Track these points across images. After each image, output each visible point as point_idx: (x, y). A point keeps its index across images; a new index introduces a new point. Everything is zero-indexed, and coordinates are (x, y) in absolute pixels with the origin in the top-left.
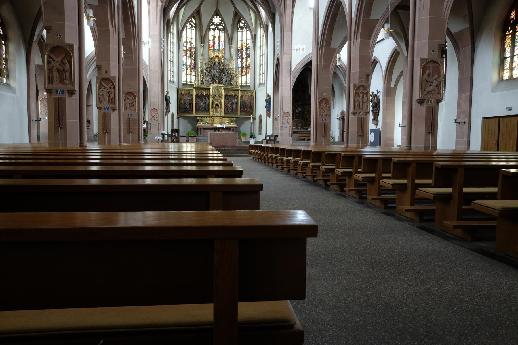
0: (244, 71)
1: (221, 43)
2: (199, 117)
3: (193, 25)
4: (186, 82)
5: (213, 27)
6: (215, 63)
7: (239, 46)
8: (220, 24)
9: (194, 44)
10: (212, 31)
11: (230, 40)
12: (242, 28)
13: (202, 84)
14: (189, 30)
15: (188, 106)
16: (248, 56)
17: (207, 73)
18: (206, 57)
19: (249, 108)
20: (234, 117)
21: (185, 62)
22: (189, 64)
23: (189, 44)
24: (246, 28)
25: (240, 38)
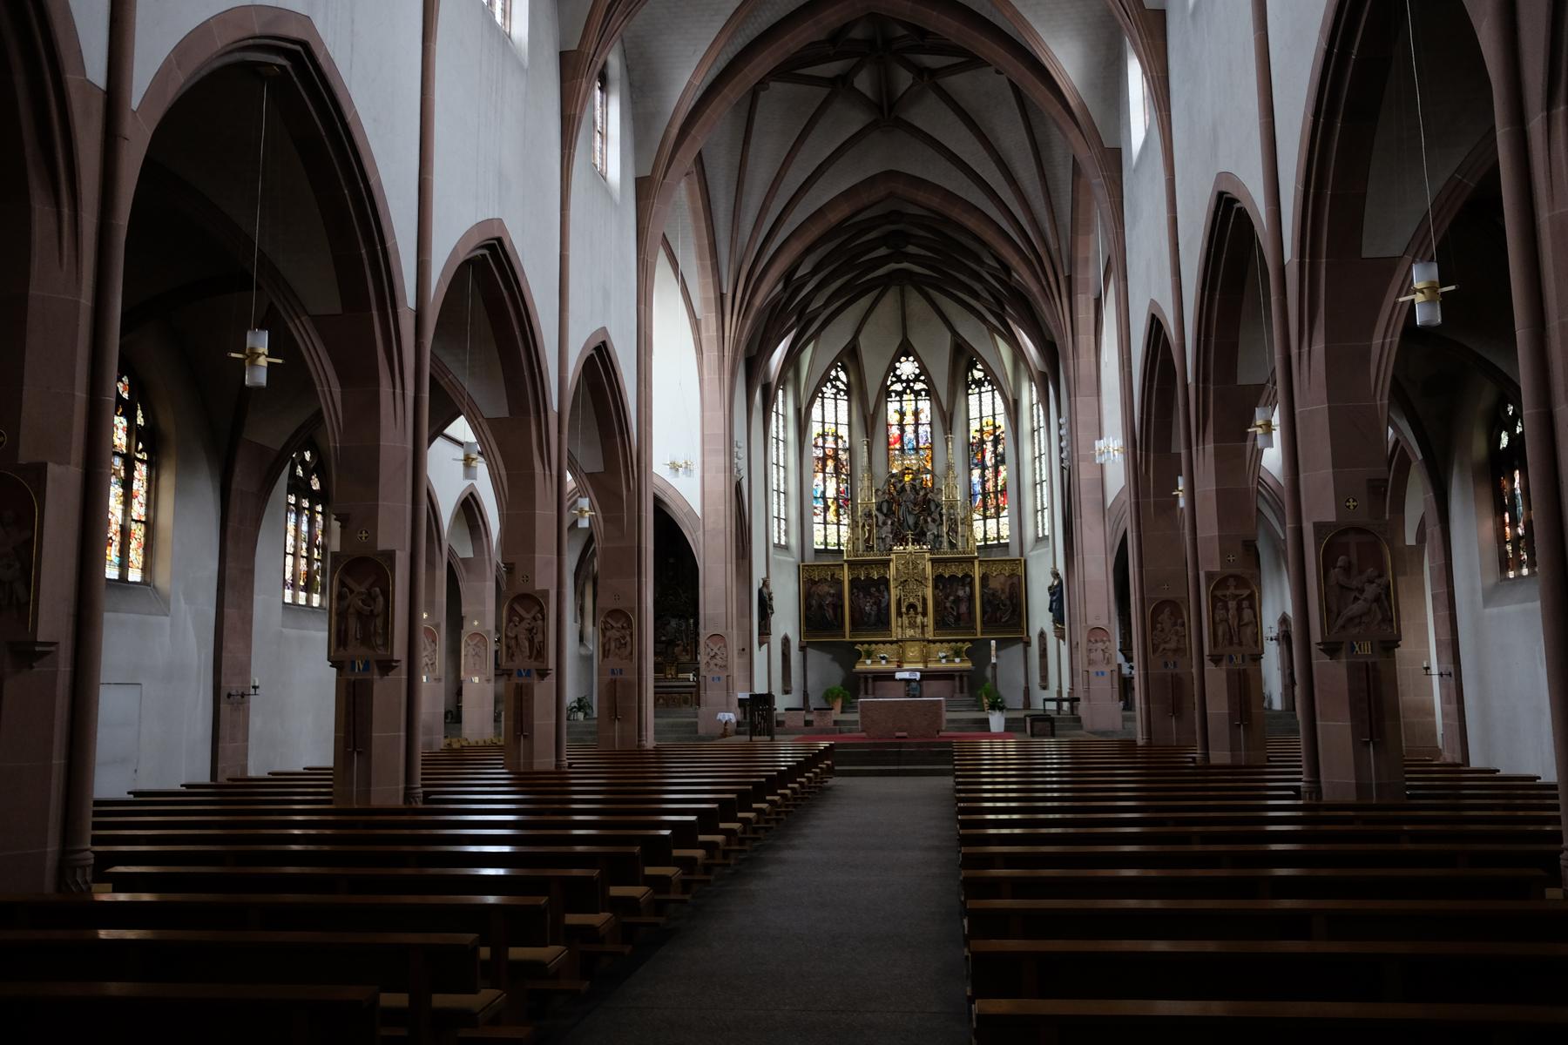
0: (991, 502)
1: (921, 429)
2: (862, 643)
3: (842, 386)
4: (826, 544)
5: (898, 387)
7: (972, 433)
8: (917, 379)
9: (846, 438)
10: (894, 397)
11: (947, 418)
12: (979, 383)
14: (829, 404)
15: (830, 613)
16: (1000, 460)
17: (881, 518)
19: (1007, 609)
20: (964, 641)
21: (821, 488)
22: (831, 493)
23: (830, 439)
24: (990, 383)
25: (974, 413)
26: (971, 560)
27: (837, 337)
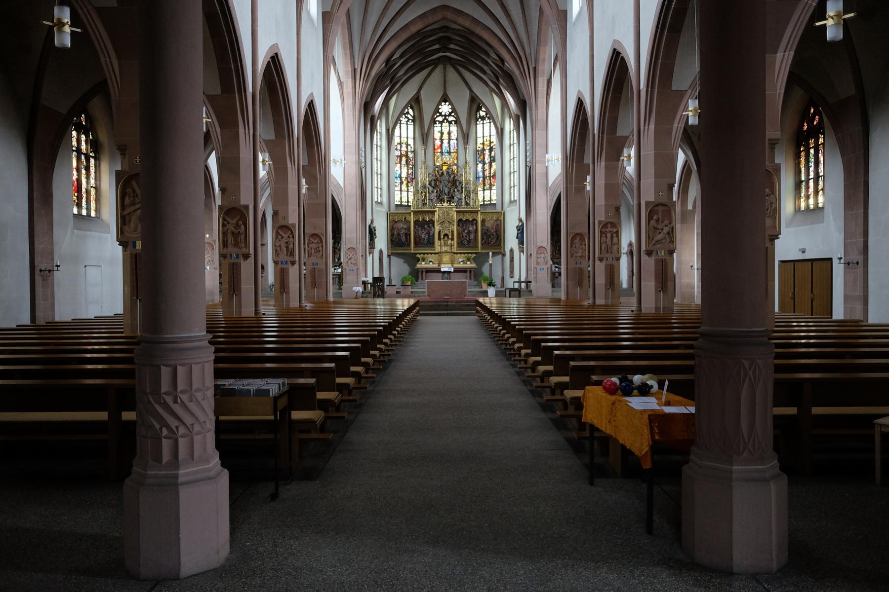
0: (487, 182)
1: (452, 142)
3: (410, 117)
5: (440, 119)
6: (443, 173)
7: (478, 145)
8: (450, 115)
10: (438, 124)
11: (465, 137)
12: (483, 118)
13: (424, 205)
15: (403, 239)
16: (493, 159)
17: (431, 189)
18: (430, 163)
19: (494, 238)
21: (399, 172)
22: (404, 175)
23: (404, 146)
24: (489, 118)
25: (480, 134)
26: (477, 212)
27: (409, 91)
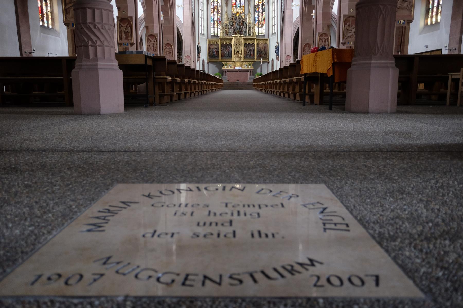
0: (260, 23)
6: (236, 18)
7: (256, 2)
9: (220, 3)
15: (215, 53)
16: (263, 10)
17: (230, 26)
18: (230, 13)
19: (264, 53)
21: (213, 18)
22: (216, 19)
23: (216, 3)
26: (254, 39)
